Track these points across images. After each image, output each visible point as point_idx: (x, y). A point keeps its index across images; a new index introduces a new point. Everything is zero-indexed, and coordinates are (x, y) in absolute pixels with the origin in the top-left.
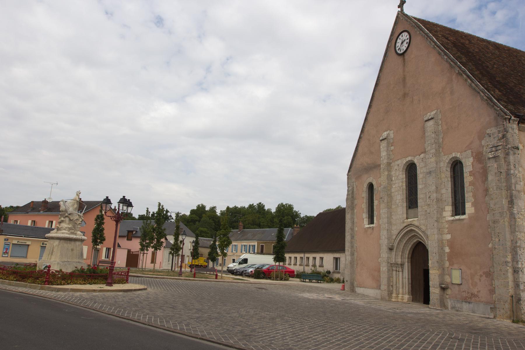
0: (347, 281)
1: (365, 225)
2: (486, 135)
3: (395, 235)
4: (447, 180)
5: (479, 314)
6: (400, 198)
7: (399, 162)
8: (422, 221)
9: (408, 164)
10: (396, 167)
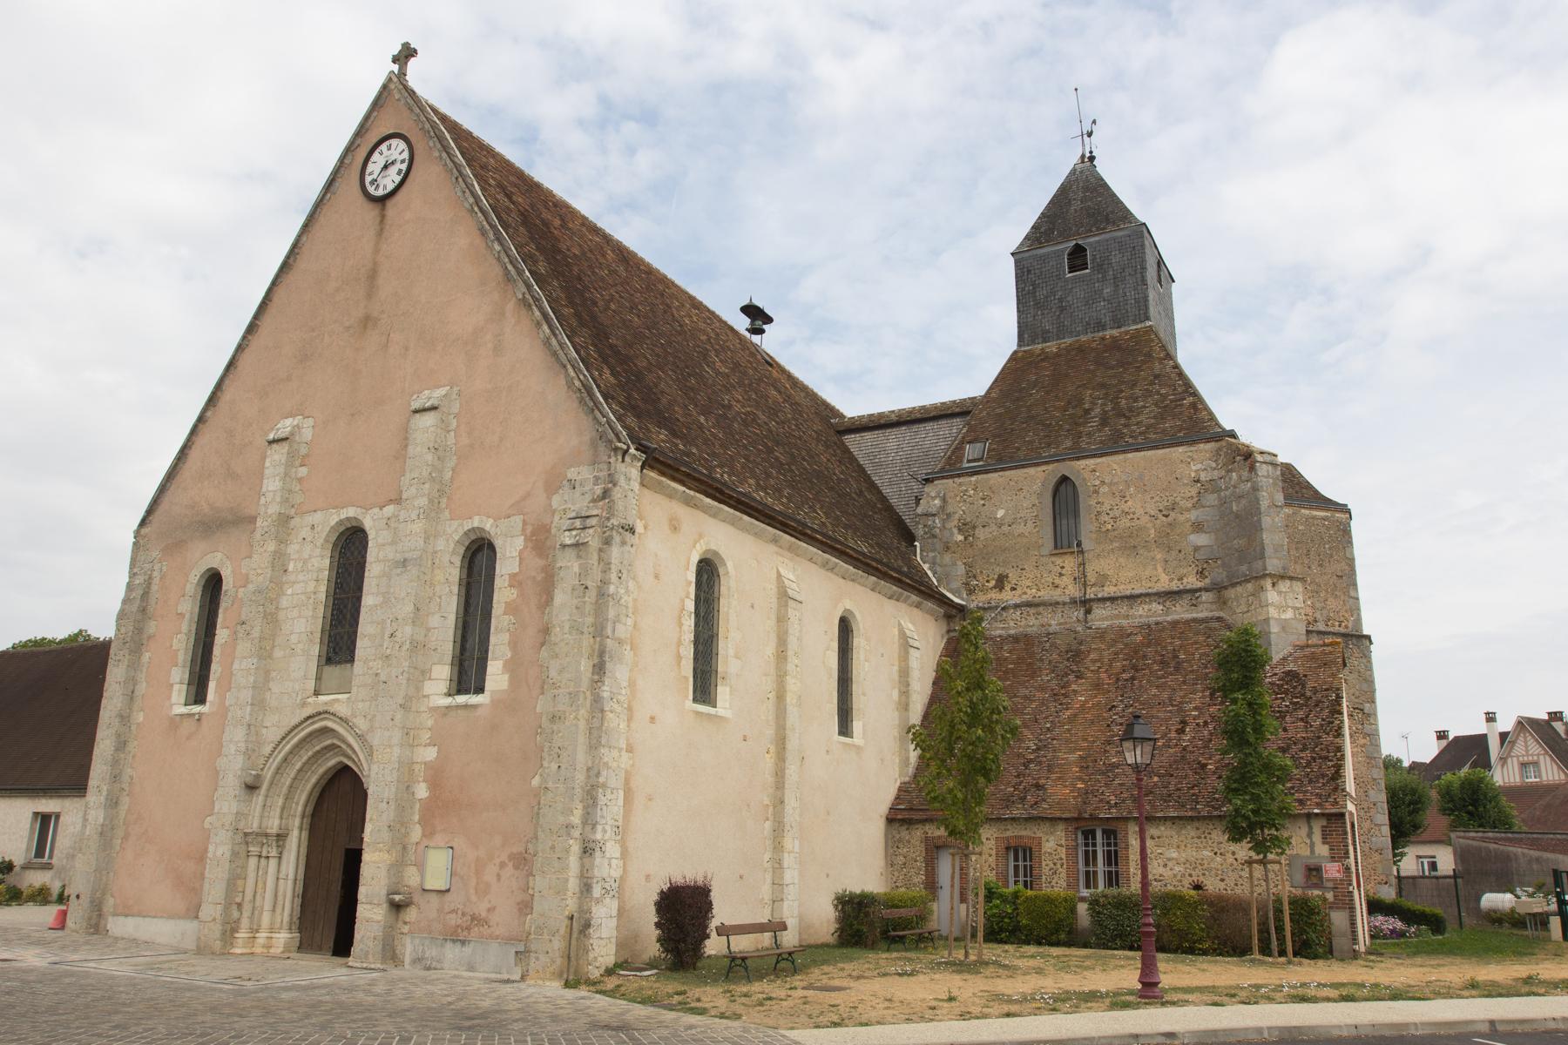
0: (78, 897)
1: (174, 707)
2: (565, 482)
3: (272, 742)
4: (448, 589)
5: (484, 972)
6: (303, 630)
7: (317, 518)
8: (360, 705)
9: (342, 529)
10: (305, 532)
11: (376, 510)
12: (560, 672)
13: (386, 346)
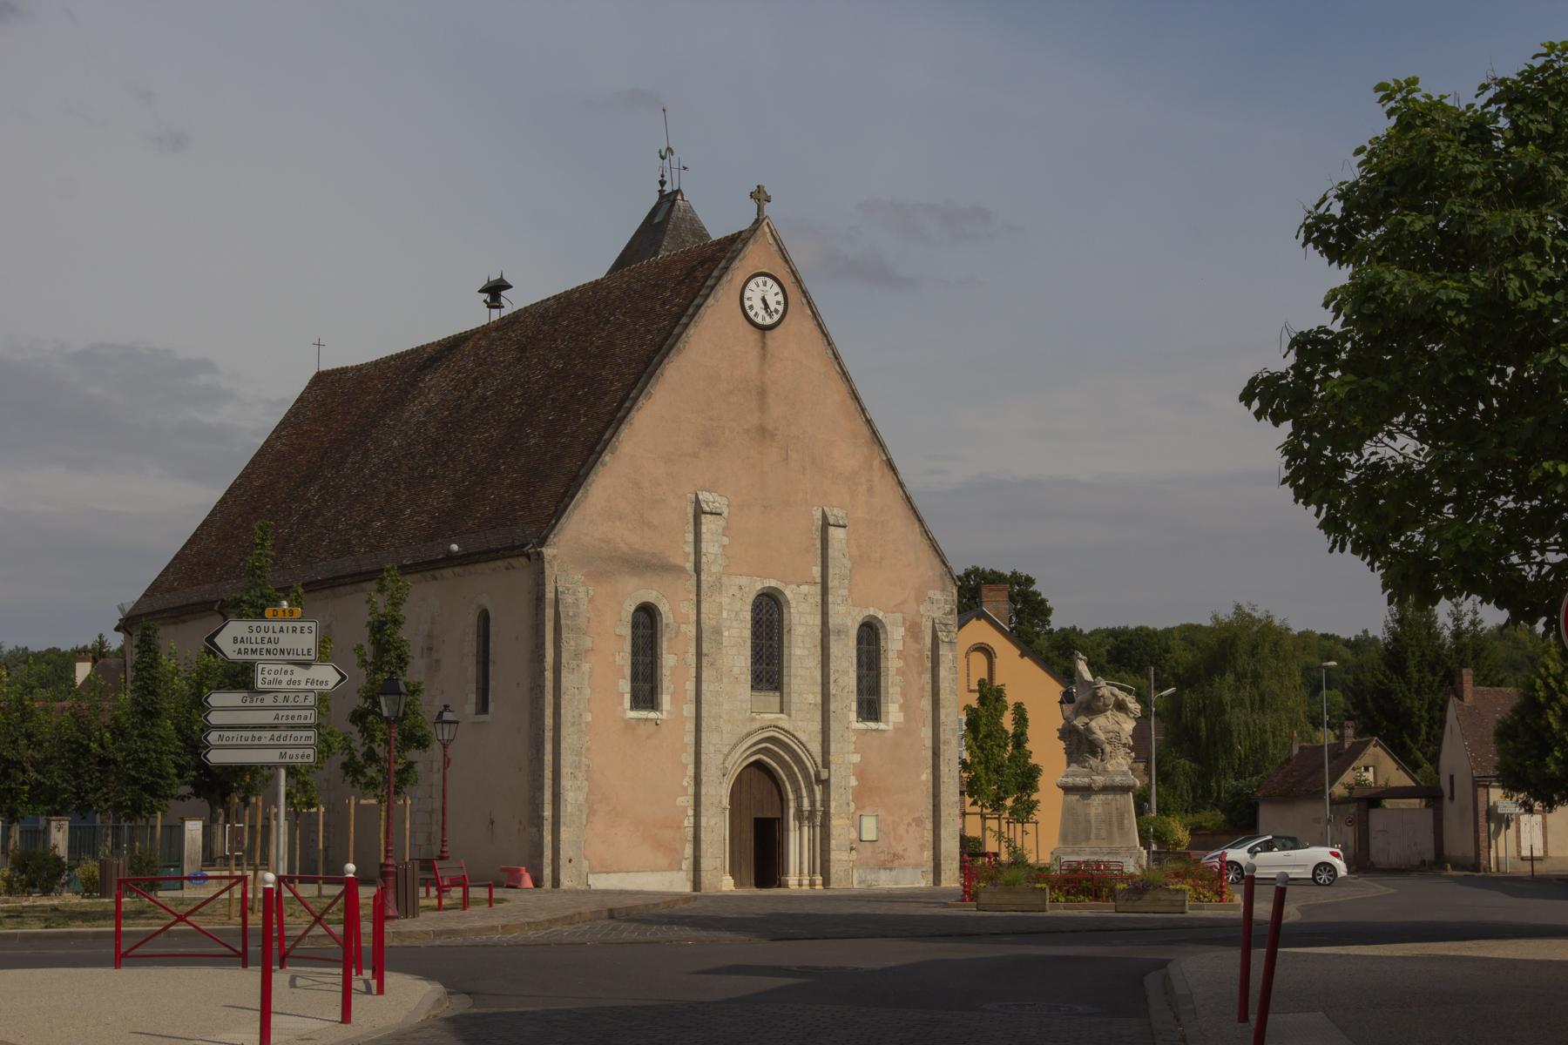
0: (570, 861)
7: (744, 581)
8: (800, 724)
10: (734, 590)
11: (794, 586)
13: (786, 459)
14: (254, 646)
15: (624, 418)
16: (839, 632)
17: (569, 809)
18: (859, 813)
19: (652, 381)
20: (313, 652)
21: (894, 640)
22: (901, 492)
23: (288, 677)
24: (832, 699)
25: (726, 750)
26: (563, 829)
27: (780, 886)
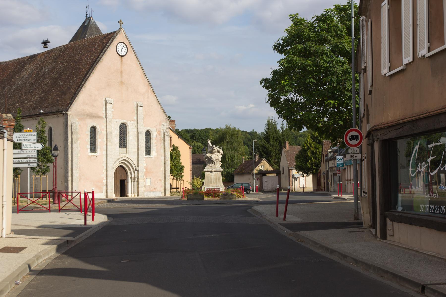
7: (117, 120)
12: (167, 154)
14: (21, 139)
15: (87, 79)
16: (141, 133)
17: (75, 178)
18: (146, 178)
19: (94, 69)
20: (36, 140)
21: (154, 136)
22: (156, 98)
23: (30, 146)
24: (139, 150)
25: (113, 163)
26: (73, 183)
27: (126, 196)
